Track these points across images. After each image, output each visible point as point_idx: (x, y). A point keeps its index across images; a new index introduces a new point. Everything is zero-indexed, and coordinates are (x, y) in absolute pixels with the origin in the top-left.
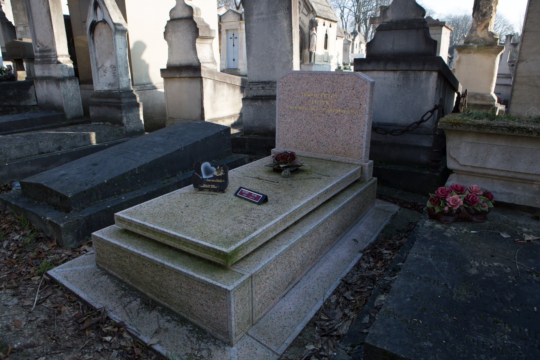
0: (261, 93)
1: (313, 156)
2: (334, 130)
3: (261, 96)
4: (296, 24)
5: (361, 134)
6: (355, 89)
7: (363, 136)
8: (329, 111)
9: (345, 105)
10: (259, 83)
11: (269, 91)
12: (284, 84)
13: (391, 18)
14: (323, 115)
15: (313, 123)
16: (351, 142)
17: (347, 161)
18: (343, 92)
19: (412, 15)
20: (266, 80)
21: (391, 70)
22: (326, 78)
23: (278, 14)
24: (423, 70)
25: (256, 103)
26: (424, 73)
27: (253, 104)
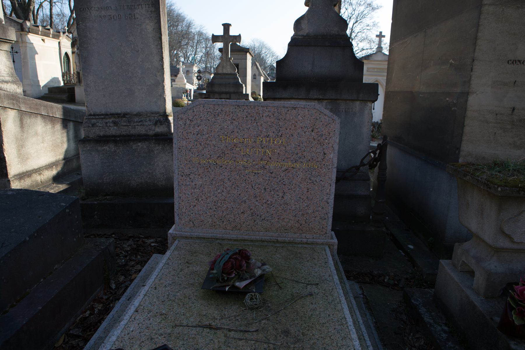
0: (113, 130)
1: (246, 237)
2: (281, 195)
3: (113, 136)
4: (165, 28)
5: (325, 198)
6: (316, 131)
7: (329, 201)
8: (272, 166)
9: (300, 155)
10: (107, 115)
11: (126, 127)
12: (188, 122)
13: (307, 32)
14: (261, 172)
15: (243, 185)
16: (310, 211)
17: (305, 240)
18: (295, 136)
19: (335, 30)
20: (119, 112)
21: (315, 99)
22: (267, 114)
23: (137, 11)
24: (357, 100)
25: (106, 148)
26: (358, 103)
27: (99, 148)
